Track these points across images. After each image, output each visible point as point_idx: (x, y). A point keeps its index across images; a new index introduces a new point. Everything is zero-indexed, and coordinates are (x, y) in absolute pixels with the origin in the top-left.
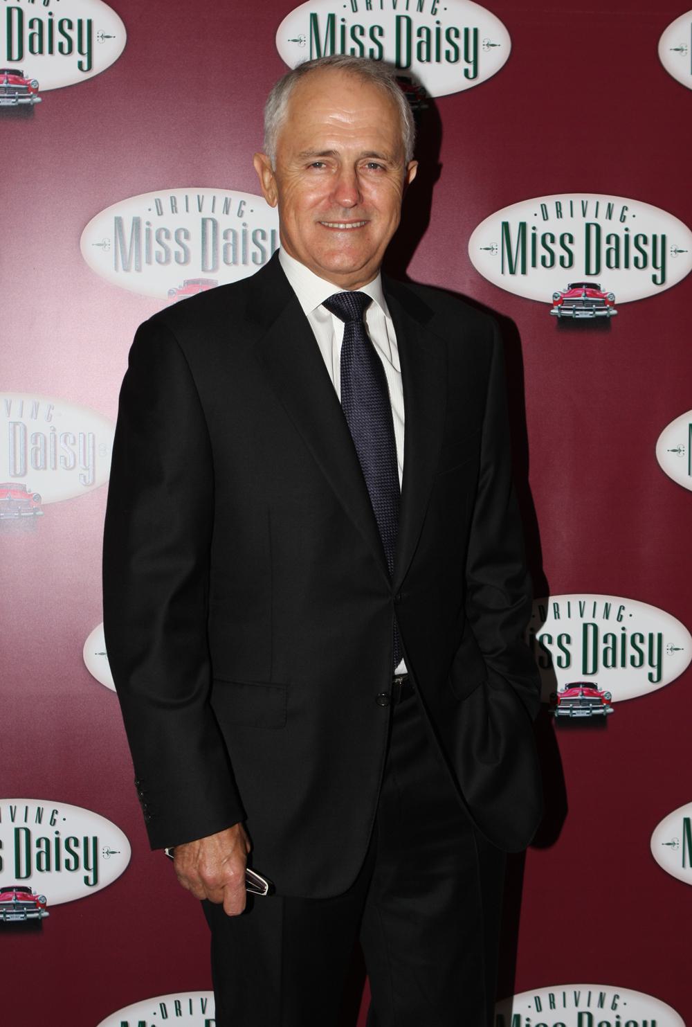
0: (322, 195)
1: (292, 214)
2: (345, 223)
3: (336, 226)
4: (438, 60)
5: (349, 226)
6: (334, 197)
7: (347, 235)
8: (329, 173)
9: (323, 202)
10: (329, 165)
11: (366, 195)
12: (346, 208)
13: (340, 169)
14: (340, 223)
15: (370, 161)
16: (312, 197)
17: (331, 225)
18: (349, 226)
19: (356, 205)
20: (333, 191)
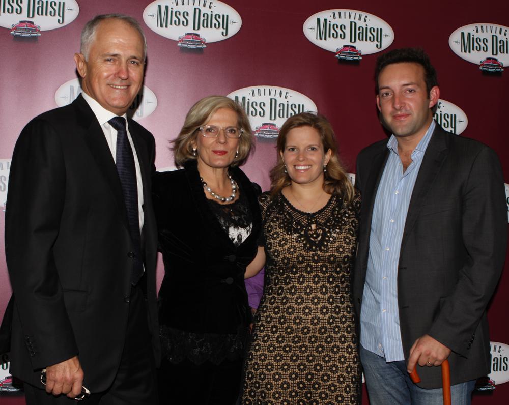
0: (111, 73)
1: (97, 80)
2: (121, 86)
3: (117, 87)
4: (46, 15)
5: (122, 88)
6: (117, 75)
7: (122, 92)
8: (115, 64)
9: (112, 77)
10: (114, 60)
11: (130, 75)
12: (123, 80)
13: (120, 63)
14: (118, 86)
15: (132, 60)
16: (105, 74)
17: (114, 86)
18: (122, 88)
19: (127, 79)
20: (117, 72)
